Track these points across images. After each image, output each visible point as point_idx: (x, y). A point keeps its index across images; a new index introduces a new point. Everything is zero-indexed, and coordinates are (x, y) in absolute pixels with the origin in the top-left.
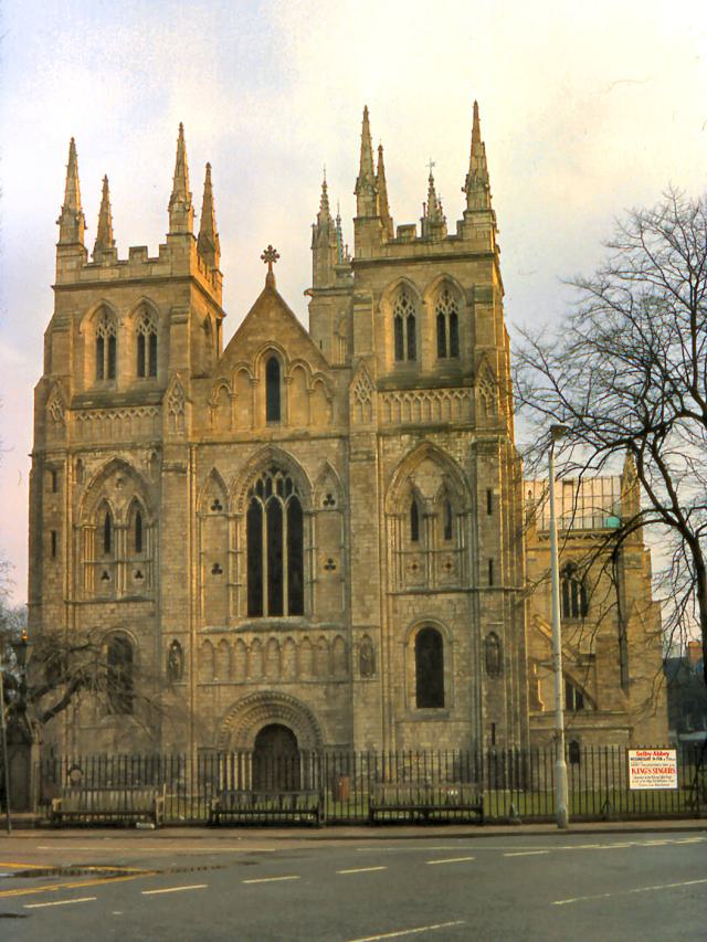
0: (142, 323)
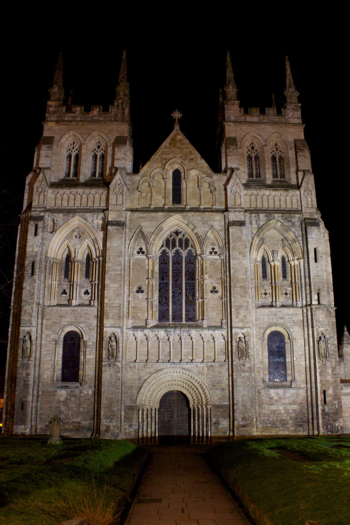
0: (95, 147)
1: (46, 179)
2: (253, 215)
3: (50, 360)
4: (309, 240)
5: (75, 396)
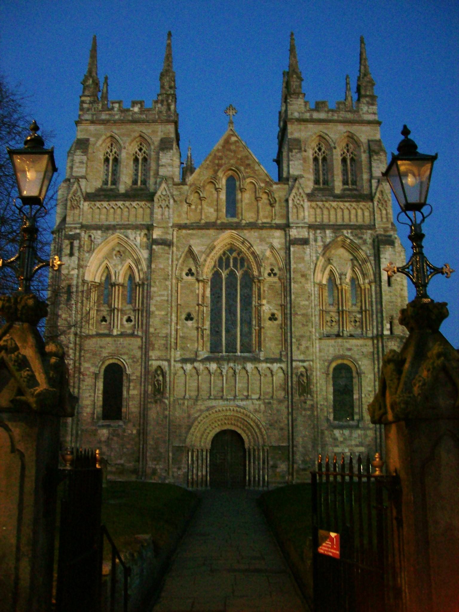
0: (137, 150)
1: (81, 190)
2: (318, 231)
3: (90, 396)
4: (383, 260)
5: (118, 435)
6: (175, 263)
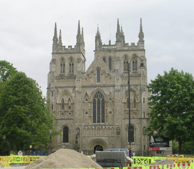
2: (124, 87)
6: (82, 97)
